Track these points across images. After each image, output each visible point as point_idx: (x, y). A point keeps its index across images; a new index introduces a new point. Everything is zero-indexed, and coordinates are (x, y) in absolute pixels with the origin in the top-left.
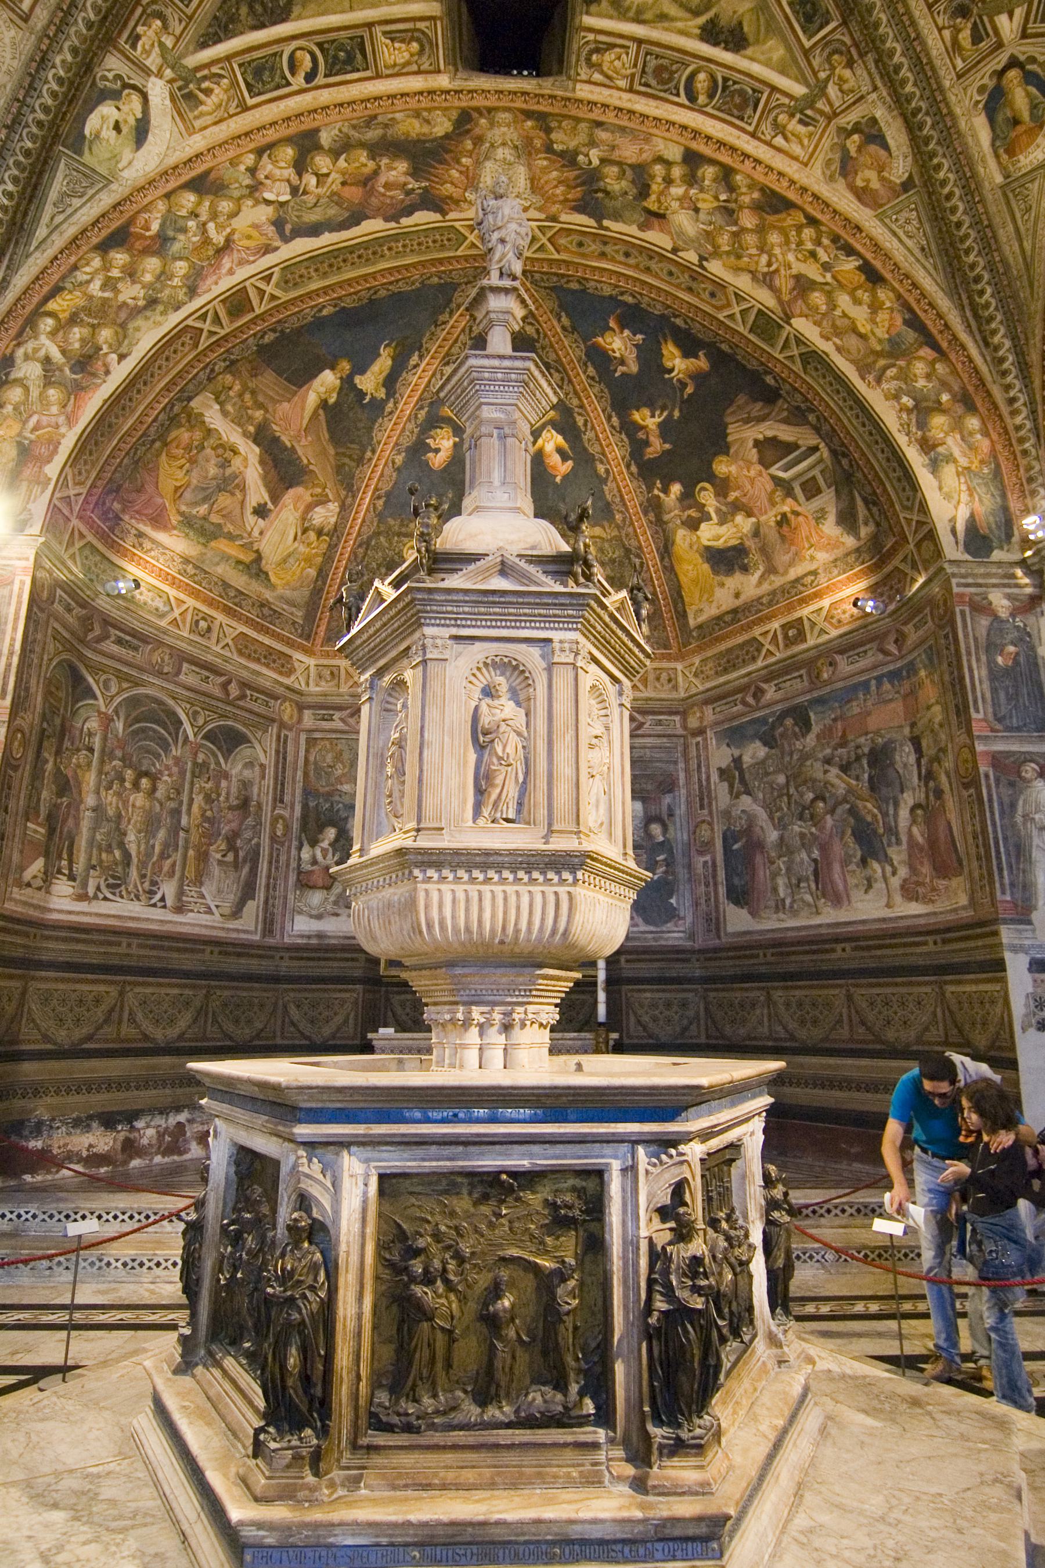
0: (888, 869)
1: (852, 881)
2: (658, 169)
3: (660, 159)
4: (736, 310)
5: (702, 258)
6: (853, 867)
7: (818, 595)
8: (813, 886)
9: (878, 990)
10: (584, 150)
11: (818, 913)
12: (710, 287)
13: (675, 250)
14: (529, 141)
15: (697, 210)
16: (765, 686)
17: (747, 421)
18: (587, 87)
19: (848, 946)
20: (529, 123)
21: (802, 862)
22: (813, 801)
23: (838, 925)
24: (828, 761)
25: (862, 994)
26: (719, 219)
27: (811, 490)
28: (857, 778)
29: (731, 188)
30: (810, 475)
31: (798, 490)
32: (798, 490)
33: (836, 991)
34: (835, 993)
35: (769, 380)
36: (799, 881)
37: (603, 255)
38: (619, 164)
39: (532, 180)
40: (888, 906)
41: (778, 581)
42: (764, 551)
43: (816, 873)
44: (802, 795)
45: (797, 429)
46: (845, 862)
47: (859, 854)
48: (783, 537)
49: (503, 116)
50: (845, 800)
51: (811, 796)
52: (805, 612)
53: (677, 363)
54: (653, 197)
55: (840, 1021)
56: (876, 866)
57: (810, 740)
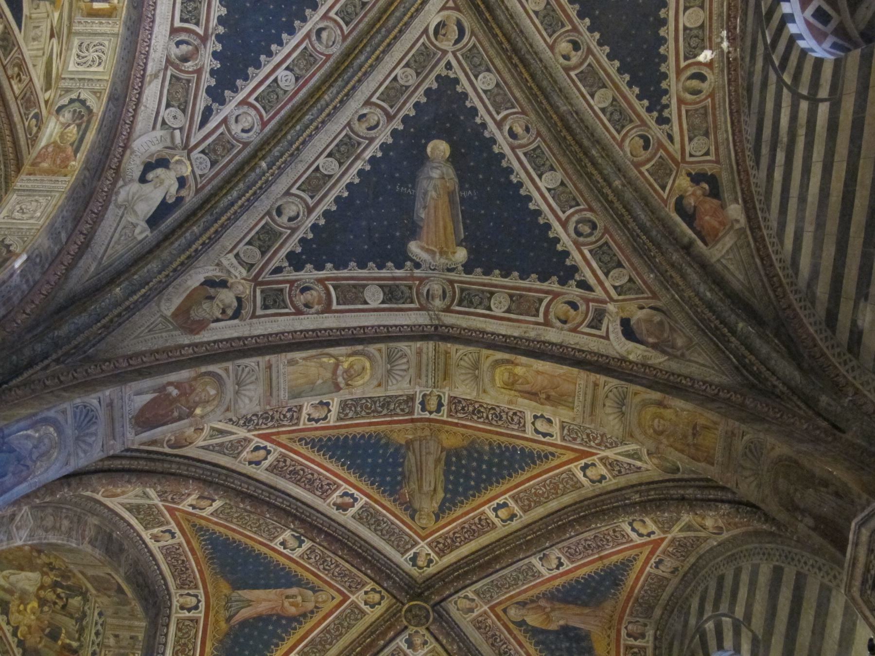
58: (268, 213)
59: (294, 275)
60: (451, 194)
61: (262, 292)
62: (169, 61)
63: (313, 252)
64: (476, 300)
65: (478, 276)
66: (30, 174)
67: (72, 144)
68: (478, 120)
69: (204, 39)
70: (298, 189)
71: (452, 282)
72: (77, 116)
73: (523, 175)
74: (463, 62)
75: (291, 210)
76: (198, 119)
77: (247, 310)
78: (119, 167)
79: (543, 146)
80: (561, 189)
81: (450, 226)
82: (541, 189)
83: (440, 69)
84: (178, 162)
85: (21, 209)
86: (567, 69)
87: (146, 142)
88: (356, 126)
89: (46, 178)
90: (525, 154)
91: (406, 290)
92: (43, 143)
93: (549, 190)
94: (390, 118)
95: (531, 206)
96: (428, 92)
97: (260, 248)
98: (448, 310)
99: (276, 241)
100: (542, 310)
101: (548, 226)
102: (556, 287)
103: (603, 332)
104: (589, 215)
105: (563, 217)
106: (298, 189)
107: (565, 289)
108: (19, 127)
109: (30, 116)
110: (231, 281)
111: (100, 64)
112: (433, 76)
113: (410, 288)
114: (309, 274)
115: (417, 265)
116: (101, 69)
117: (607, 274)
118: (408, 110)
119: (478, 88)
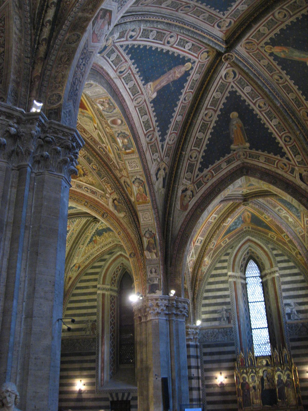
58: (188, 159)
59: (202, 174)
60: (241, 128)
62: (148, 143)
63: (204, 165)
64: (254, 157)
65: (254, 151)
68: (247, 104)
69: (154, 130)
70: (194, 147)
71: (246, 152)
72: (140, 183)
73: (265, 121)
74: (237, 84)
75: (194, 156)
76: (161, 150)
77: (195, 192)
79: (271, 110)
80: (279, 125)
81: (242, 137)
82: (272, 125)
83: (230, 89)
86: (278, 84)
87: (153, 169)
88: (205, 118)
89: (144, 205)
90: (265, 113)
91: (233, 159)
92: (136, 194)
93: (275, 125)
94: (215, 111)
95: (269, 131)
96: (227, 98)
98: (246, 158)
99: (194, 166)
100: (276, 164)
101: (275, 138)
102: (279, 158)
103: (294, 175)
104: (288, 134)
105: (280, 135)
106: (194, 147)
107: (282, 159)
108: (94, 147)
109: (99, 146)
112: (227, 92)
113: (234, 157)
114: (206, 171)
115: (234, 151)
116: (138, 168)
117: (295, 156)
118: (221, 106)
119: (245, 92)
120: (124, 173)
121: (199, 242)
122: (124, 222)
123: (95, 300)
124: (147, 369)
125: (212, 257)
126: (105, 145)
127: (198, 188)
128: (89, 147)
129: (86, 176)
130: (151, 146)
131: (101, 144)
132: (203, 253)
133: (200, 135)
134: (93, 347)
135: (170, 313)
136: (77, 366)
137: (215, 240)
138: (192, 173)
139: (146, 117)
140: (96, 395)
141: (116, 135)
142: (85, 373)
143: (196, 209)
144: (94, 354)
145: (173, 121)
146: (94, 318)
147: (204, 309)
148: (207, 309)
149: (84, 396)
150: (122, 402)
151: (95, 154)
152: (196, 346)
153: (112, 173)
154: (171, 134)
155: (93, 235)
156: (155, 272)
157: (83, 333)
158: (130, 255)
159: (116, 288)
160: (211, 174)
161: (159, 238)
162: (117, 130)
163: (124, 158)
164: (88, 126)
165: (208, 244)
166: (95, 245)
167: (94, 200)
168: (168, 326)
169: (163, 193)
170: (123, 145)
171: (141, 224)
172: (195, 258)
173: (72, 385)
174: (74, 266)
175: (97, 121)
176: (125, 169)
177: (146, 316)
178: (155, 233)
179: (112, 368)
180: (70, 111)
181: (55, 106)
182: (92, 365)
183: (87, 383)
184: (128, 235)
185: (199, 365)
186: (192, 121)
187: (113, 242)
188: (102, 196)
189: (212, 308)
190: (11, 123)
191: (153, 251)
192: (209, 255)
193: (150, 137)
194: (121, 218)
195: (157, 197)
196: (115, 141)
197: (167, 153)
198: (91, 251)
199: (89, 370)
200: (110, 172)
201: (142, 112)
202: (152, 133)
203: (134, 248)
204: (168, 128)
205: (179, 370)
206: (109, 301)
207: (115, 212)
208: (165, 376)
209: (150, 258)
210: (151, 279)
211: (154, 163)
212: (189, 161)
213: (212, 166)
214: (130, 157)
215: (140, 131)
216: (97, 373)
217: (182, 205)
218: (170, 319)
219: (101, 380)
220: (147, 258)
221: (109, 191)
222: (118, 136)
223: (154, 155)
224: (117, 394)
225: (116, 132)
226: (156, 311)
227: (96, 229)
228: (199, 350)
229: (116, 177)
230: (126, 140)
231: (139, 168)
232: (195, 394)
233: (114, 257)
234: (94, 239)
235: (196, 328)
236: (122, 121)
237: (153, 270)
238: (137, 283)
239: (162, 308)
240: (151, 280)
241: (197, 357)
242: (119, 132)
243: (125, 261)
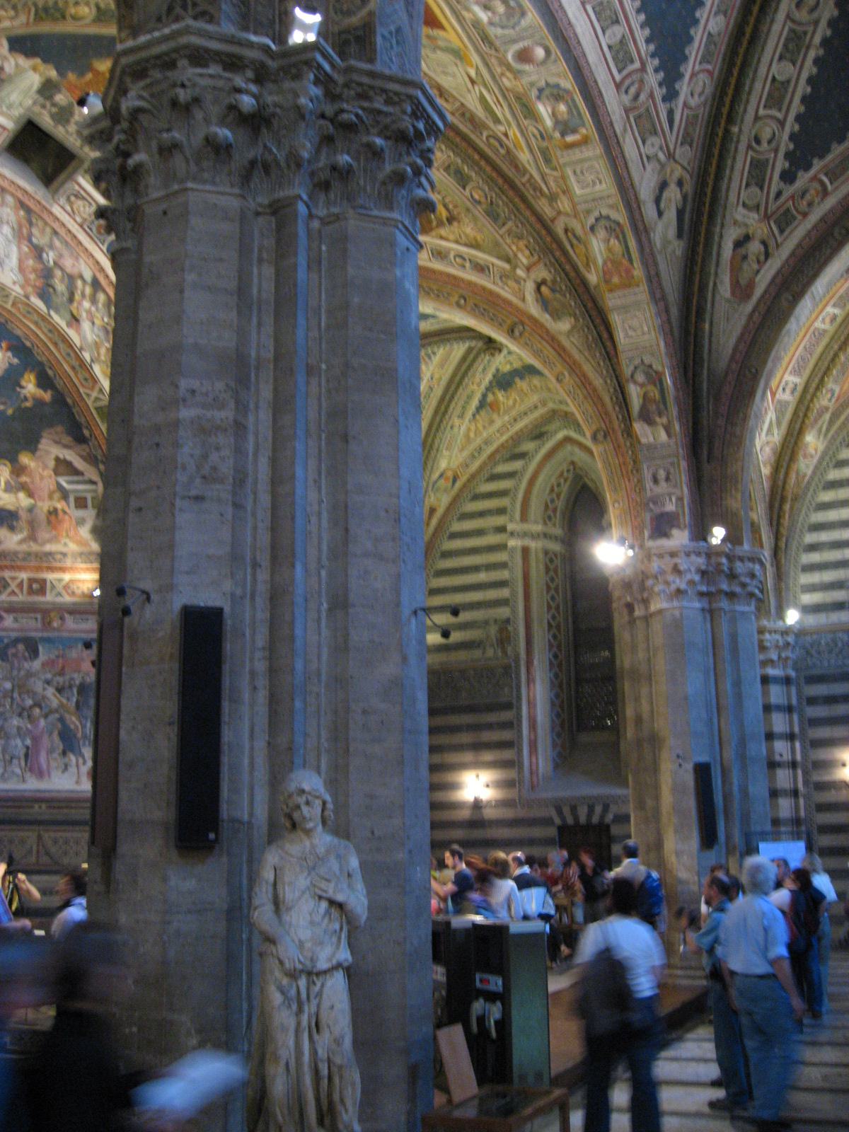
0: (81, 761)
1: (53, 764)
2: (79, 283)
3: (81, 277)
4: (94, 394)
5: (92, 360)
6: (55, 755)
7: (63, 570)
8: (23, 763)
9: (60, 834)
10: (46, 249)
11: (24, 781)
12: (87, 376)
13: (81, 349)
14: (20, 226)
15: (93, 323)
16: (4, 615)
17: (57, 442)
18: (59, 209)
19: (44, 806)
20: (22, 213)
21: (16, 746)
22: (31, 707)
23: (39, 791)
24: (48, 682)
25: (48, 836)
26: (102, 334)
27: (81, 503)
28: (68, 699)
29: (109, 316)
30: (83, 495)
31: (72, 499)
32: (72, 499)
33: (31, 834)
34: (30, 835)
35: (86, 433)
36: (12, 758)
37: (36, 324)
38: (62, 269)
39: (20, 261)
40: (77, 782)
41: (34, 547)
42: (32, 524)
43: (26, 756)
44: (23, 700)
45: (88, 466)
46: (50, 751)
47: (61, 747)
48: (49, 522)
49: (9, 199)
50: (56, 711)
51: (29, 702)
52: (50, 576)
53: (30, 386)
54: (75, 304)
55: (30, 852)
56: (73, 758)
57: (37, 664)
58: (749, 147)
61: (775, 222)
62: (627, 111)
63: (799, 160)
66: (611, 291)
67: (623, 255)
69: (643, 69)
72: (610, 230)
75: (766, 134)
77: (772, 243)
78: (645, 227)
84: (672, 171)
85: (630, 327)
87: (645, 186)
92: (600, 262)
97: (757, 184)
106: (765, 107)
108: (473, 137)
109: (485, 134)
110: (751, 232)
111: (600, 182)
114: (803, 179)
120: (564, 204)
121: (788, 391)
122: (573, 345)
123: (503, 565)
124: (655, 741)
125: (828, 430)
126: (502, 128)
127: (782, 231)
128: (458, 140)
129: (455, 224)
130: (638, 118)
131: (491, 125)
132: (800, 421)
133: (783, 70)
134: (506, 690)
135: (713, 589)
136: (465, 738)
137: (836, 381)
138: (761, 188)
139: (618, 31)
140: (521, 813)
141: (534, 93)
142: (488, 756)
143: (777, 296)
144: (508, 706)
145: (698, 34)
146: (504, 612)
147: (806, 579)
148: (815, 578)
149: (489, 814)
150: (588, 827)
151: (476, 157)
152: (787, 681)
153: (529, 206)
154: (693, 75)
155: (487, 389)
156: (667, 479)
157: (477, 653)
158: (594, 438)
159: (558, 531)
160: (820, 188)
161: (674, 384)
162: (534, 78)
163: (561, 161)
164: (450, 79)
165: (814, 395)
166: (495, 416)
167: (484, 289)
168: (709, 626)
169: (679, 253)
170: (557, 123)
171: (620, 348)
172: (777, 437)
173: (455, 786)
174: (441, 476)
175: (475, 59)
176: (564, 192)
177: (646, 602)
178: (660, 369)
179: (559, 742)
180: (399, 30)
181: (355, 20)
182: (506, 735)
183: (492, 782)
184: (584, 381)
185: (796, 730)
186: (756, 30)
187: (544, 403)
188: (504, 276)
189: (828, 576)
190: (239, 81)
191: (658, 420)
192: (817, 426)
193: (633, 90)
194: (560, 333)
195: (662, 267)
196: (531, 114)
197: (687, 134)
198: (485, 435)
199: (498, 745)
200: (522, 206)
201: (607, 17)
202: (635, 77)
203: (604, 414)
204: (686, 58)
205: (742, 743)
206: (542, 567)
207: (545, 318)
208: (703, 758)
209: (651, 439)
210: (655, 500)
211: (649, 167)
212: (750, 153)
213: (822, 163)
214: (577, 154)
215: (603, 74)
216: (520, 752)
217: (735, 284)
218: (714, 605)
219: (531, 773)
220: (644, 440)
221: (525, 261)
222: (539, 98)
223: (648, 142)
224: (574, 809)
225: (532, 84)
226: (673, 587)
227: (492, 370)
228: (793, 690)
229: (540, 219)
230: (562, 108)
231: (606, 186)
232: (785, 807)
233: (549, 445)
234: (490, 398)
235: (786, 632)
236: (548, 52)
237: (662, 474)
238: (617, 512)
239: (689, 577)
240: (655, 503)
241: (790, 709)
242: (543, 83)
243: (580, 456)
